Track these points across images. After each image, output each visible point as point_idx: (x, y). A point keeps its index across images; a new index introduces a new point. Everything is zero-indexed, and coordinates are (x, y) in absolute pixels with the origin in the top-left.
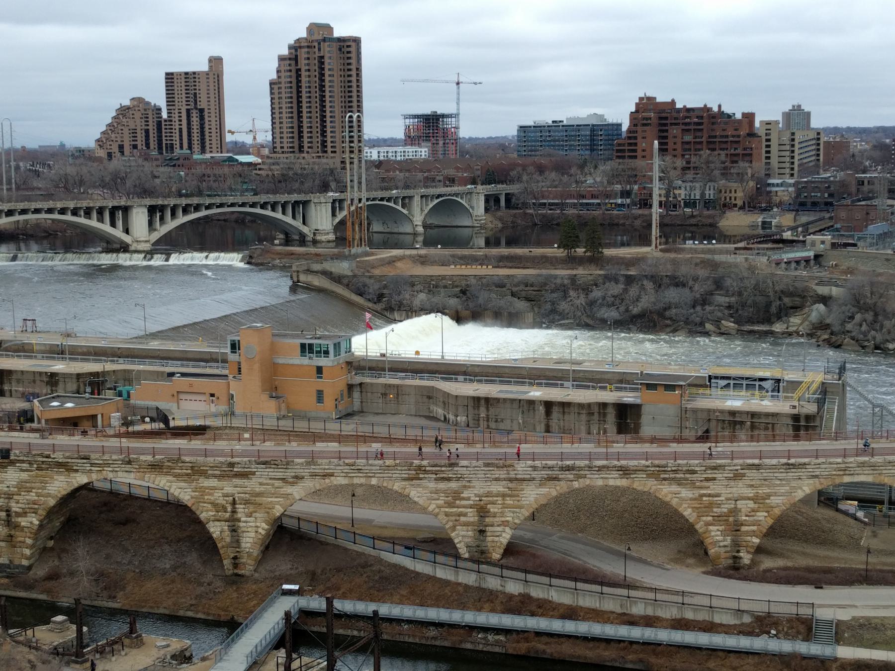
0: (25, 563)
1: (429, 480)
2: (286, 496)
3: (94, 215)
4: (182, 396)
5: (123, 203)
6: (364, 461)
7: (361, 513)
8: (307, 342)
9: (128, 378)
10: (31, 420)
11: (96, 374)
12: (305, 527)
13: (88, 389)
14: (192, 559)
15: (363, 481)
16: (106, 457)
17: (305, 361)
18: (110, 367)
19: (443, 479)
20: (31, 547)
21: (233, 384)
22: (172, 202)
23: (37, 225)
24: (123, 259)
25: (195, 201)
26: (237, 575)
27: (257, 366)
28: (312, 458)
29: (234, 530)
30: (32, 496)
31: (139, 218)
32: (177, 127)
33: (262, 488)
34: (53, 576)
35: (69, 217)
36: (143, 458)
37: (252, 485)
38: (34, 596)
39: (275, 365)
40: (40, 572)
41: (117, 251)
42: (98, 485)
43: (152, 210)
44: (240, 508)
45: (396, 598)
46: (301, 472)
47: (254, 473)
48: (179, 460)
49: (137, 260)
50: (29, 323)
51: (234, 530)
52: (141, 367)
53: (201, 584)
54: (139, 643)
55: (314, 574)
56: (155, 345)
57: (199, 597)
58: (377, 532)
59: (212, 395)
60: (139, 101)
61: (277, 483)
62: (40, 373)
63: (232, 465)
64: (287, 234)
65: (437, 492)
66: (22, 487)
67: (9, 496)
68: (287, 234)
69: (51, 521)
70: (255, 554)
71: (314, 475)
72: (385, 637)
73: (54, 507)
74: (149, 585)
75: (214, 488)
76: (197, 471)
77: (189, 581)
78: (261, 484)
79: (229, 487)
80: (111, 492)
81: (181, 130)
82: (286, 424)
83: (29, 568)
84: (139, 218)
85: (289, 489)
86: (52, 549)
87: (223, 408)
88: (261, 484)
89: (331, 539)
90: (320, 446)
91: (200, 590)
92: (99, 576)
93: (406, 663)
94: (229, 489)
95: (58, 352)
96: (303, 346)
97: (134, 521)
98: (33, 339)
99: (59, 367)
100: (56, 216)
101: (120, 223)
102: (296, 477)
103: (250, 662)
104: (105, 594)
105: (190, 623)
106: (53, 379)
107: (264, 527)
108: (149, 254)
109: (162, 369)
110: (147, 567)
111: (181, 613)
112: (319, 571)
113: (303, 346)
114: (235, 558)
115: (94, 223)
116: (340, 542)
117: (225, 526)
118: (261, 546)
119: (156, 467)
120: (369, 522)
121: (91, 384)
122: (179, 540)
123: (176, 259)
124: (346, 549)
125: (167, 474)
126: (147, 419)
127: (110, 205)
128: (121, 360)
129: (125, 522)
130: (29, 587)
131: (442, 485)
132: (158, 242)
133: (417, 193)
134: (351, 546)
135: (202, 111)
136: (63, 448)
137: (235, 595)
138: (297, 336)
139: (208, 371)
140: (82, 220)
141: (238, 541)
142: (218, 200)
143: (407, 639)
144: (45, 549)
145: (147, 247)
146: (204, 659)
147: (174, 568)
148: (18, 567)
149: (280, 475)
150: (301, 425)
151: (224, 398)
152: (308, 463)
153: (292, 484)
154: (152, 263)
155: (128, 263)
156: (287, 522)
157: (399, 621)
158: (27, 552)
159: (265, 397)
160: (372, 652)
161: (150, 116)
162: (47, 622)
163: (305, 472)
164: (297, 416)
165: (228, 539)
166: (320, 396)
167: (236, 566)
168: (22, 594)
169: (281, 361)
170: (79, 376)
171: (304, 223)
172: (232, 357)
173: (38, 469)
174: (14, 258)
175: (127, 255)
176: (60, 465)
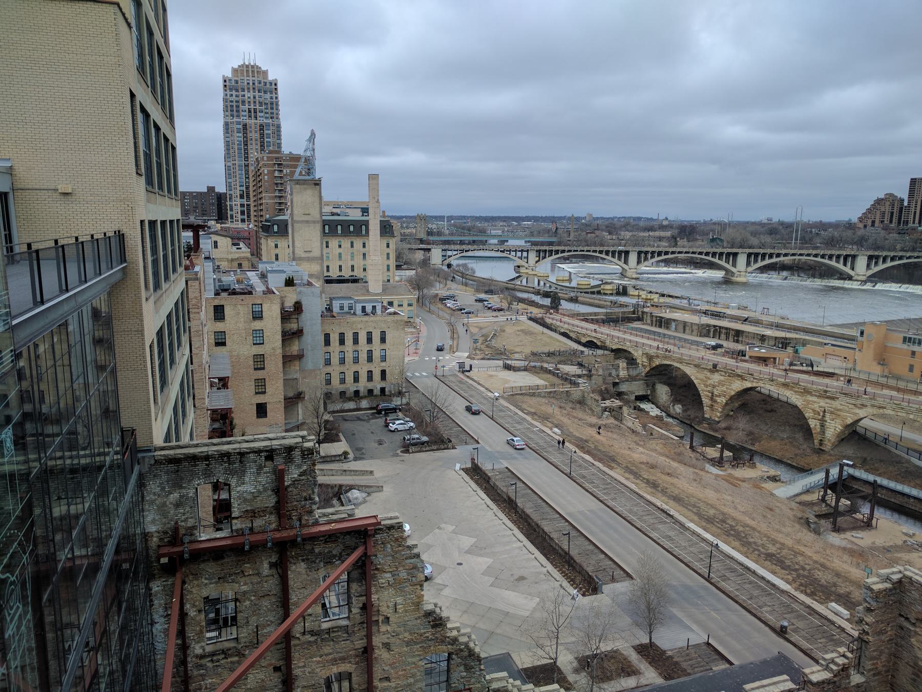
0: (717, 419)
2: (856, 414)
3: (834, 258)
4: (828, 356)
5: (853, 253)
6: (906, 404)
7: (908, 434)
8: (908, 336)
9: (804, 343)
10: (745, 356)
11: (786, 339)
12: (869, 434)
13: (780, 346)
14: (799, 436)
15: (904, 415)
16: (762, 376)
17: (905, 347)
18: (789, 335)
20: (721, 412)
21: (857, 353)
22: (884, 254)
23: (805, 263)
24: (847, 284)
25: (900, 254)
26: (820, 449)
27: (872, 346)
28: (874, 397)
29: (822, 426)
30: (724, 388)
31: (861, 262)
32: (913, 211)
33: (842, 407)
34: (728, 428)
35: (819, 259)
36: (779, 379)
37: (836, 404)
38: (717, 435)
39: (886, 346)
40: (723, 425)
41: (844, 279)
42: (763, 390)
43: (870, 258)
44: (827, 415)
45: (912, 484)
46: (865, 403)
47: (838, 398)
48: (797, 384)
49: (855, 285)
50: (766, 310)
51: (822, 426)
52: (807, 338)
53: (799, 449)
54: (753, 466)
55: (865, 459)
56: (828, 329)
57: (796, 455)
58: (909, 446)
59: (845, 358)
60: (891, 195)
61: (851, 406)
62: (757, 334)
63: (826, 391)
66: (721, 383)
67: (714, 387)
69: (732, 402)
70: (833, 440)
71: (873, 406)
72: (879, 495)
73: (734, 395)
74: (773, 443)
75: (815, 402)
76: (806, 391)
77: (794, 446)
78: (841, 405)
79: (823, 403)
80: (769, 396)
81: (915, 213)
82: (883, 380)
83: (719, 422)
84: (861, 262)
85: (857, 411)
86: (732, 416)
87: (850, 366)
88: (841, 405)
89: (883, 444)
90: (886, 392)
91: (798, 452)
92: (750, 433)
93: (917, 523)
94: (822, 404)
95: (771, 325)
96: (905, 338)
97: (775, 411)
98: (764, 318)
99: (768, 332)
100: (812, 258)
101: (849, 264)
102: (863, 405)
103: (804, 488)
104: (750, 442)
105: (779, 462)
106: (763, 338)
107: (839, 428)
108: (864, 282)
109: (822, 341)
110: (775, 435)
111: (785, 460)
112: (869, 458)
113: (905, 338)
114: (821, 440)
115: (833, 263)
116: (888, 447)
117: (818, 423)
118: (838, 437)
119: (785, 385)
120: (914, 441)
121: (782, 343)
122: (795, 425)
123: (880, 286)
124: (890, 452)
125: (791, 390)
126: (804, 365)
127: (845, 254)
128: (802, 333)
129: (772, 411)
130: (716, 431)
132: (873, 276)
134: (894, 450)
136: (742, 368)
137: (816, 459)
138: (905, 332)
139: (849, 345)
140: (826, 261)
141: (824, 432)
142: (916, 254)
143: (910, 507)
144: (728, 415)
145: (864, 278)
146: (783, 482)
147: (788, 438)
148: (714, 420)
149: (853, 402)
150: (902, 384)
151: (851, 361)
152: (870, 399)
153: (860, 408)
154: (865, 287)
155: (850, 286)
156: (858, 429)
157: (909, 496)
158: (719, 414)
159: (875, 363)
160: (870, 501)
161: (896, 204)
162: (714, 446)
163: (868, 404)
164: (898, 378)
165: (819, 430)
166: (911, 368)
167: (821, 444)
168: (712, 433)
169: (889, 345)
170: (776, 338)
172: (860, 338)
173: (729, 376)
174: (786, 279)
175: (850, 282)
176: (739, 376)
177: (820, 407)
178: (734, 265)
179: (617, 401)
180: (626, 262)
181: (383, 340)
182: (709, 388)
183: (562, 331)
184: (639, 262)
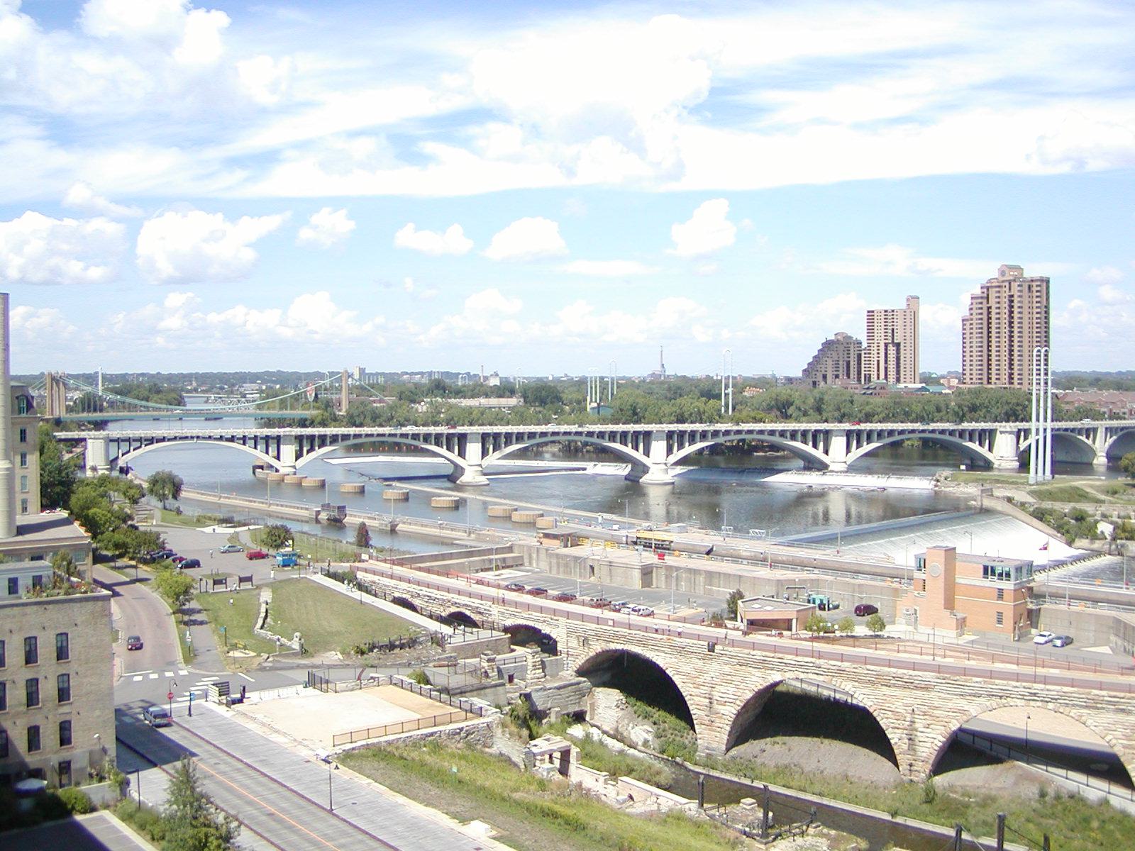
1: (1108, 710)
19: (1123, 711)
31: (838, 443)
32: (876, 359)
64: (972, 460)
65: (1116, 723)
68: (972, 460)
84: (838, 443)
88: (940, 698)
96: (986, 569)
101: (821, 445)
131: (1121, 717)
133: (1102, 425)
135: (898, 345)
165: (905, 747)
171: (990, 449)
177: (906, 705)
178: (647, 453)
179: (559, 738)
180: (462, 454)
181: (62, 654)
182: (704, 690)
183: (397, 595)
184: (484, 453)
